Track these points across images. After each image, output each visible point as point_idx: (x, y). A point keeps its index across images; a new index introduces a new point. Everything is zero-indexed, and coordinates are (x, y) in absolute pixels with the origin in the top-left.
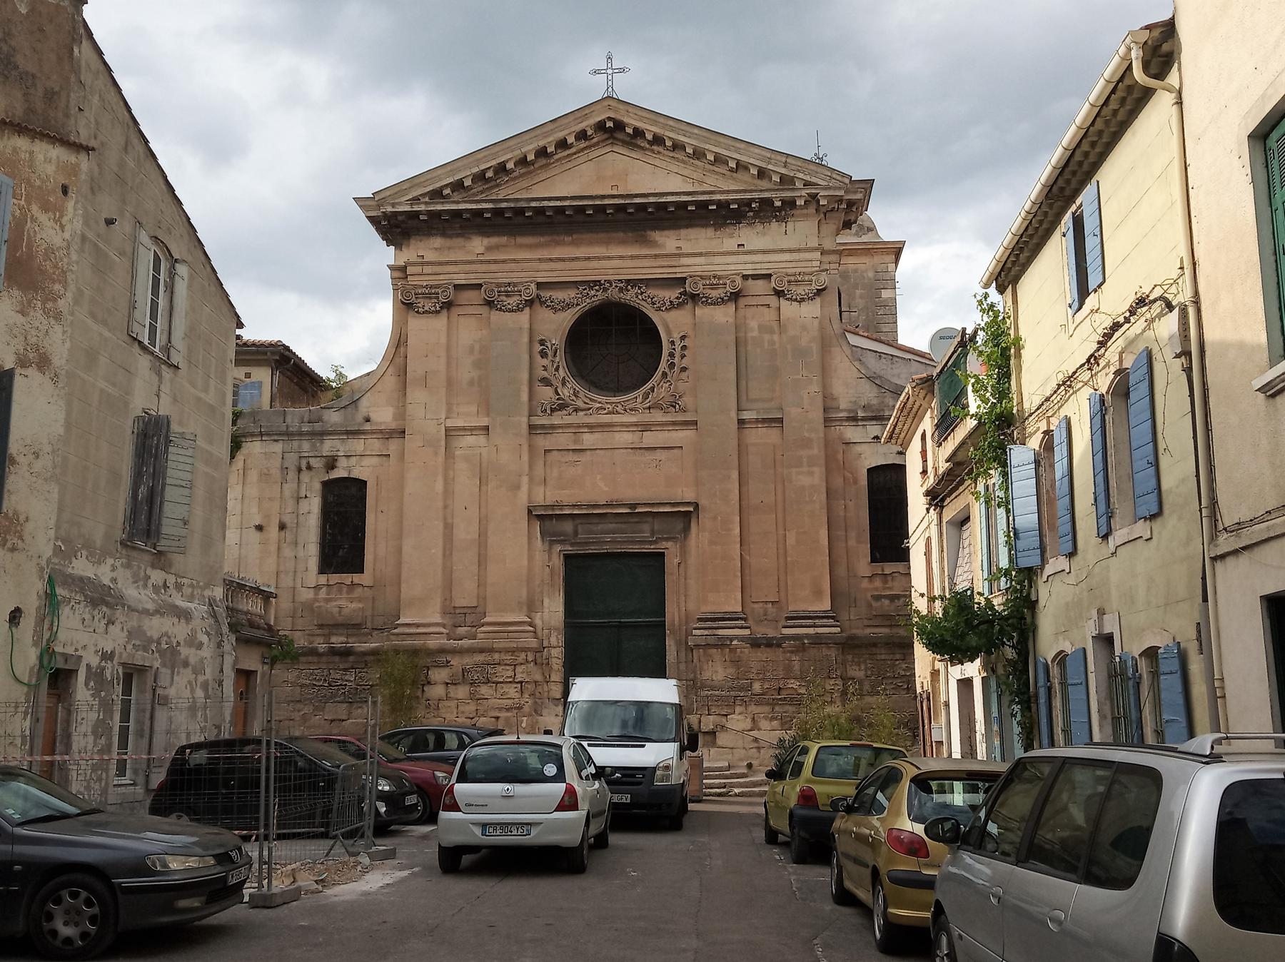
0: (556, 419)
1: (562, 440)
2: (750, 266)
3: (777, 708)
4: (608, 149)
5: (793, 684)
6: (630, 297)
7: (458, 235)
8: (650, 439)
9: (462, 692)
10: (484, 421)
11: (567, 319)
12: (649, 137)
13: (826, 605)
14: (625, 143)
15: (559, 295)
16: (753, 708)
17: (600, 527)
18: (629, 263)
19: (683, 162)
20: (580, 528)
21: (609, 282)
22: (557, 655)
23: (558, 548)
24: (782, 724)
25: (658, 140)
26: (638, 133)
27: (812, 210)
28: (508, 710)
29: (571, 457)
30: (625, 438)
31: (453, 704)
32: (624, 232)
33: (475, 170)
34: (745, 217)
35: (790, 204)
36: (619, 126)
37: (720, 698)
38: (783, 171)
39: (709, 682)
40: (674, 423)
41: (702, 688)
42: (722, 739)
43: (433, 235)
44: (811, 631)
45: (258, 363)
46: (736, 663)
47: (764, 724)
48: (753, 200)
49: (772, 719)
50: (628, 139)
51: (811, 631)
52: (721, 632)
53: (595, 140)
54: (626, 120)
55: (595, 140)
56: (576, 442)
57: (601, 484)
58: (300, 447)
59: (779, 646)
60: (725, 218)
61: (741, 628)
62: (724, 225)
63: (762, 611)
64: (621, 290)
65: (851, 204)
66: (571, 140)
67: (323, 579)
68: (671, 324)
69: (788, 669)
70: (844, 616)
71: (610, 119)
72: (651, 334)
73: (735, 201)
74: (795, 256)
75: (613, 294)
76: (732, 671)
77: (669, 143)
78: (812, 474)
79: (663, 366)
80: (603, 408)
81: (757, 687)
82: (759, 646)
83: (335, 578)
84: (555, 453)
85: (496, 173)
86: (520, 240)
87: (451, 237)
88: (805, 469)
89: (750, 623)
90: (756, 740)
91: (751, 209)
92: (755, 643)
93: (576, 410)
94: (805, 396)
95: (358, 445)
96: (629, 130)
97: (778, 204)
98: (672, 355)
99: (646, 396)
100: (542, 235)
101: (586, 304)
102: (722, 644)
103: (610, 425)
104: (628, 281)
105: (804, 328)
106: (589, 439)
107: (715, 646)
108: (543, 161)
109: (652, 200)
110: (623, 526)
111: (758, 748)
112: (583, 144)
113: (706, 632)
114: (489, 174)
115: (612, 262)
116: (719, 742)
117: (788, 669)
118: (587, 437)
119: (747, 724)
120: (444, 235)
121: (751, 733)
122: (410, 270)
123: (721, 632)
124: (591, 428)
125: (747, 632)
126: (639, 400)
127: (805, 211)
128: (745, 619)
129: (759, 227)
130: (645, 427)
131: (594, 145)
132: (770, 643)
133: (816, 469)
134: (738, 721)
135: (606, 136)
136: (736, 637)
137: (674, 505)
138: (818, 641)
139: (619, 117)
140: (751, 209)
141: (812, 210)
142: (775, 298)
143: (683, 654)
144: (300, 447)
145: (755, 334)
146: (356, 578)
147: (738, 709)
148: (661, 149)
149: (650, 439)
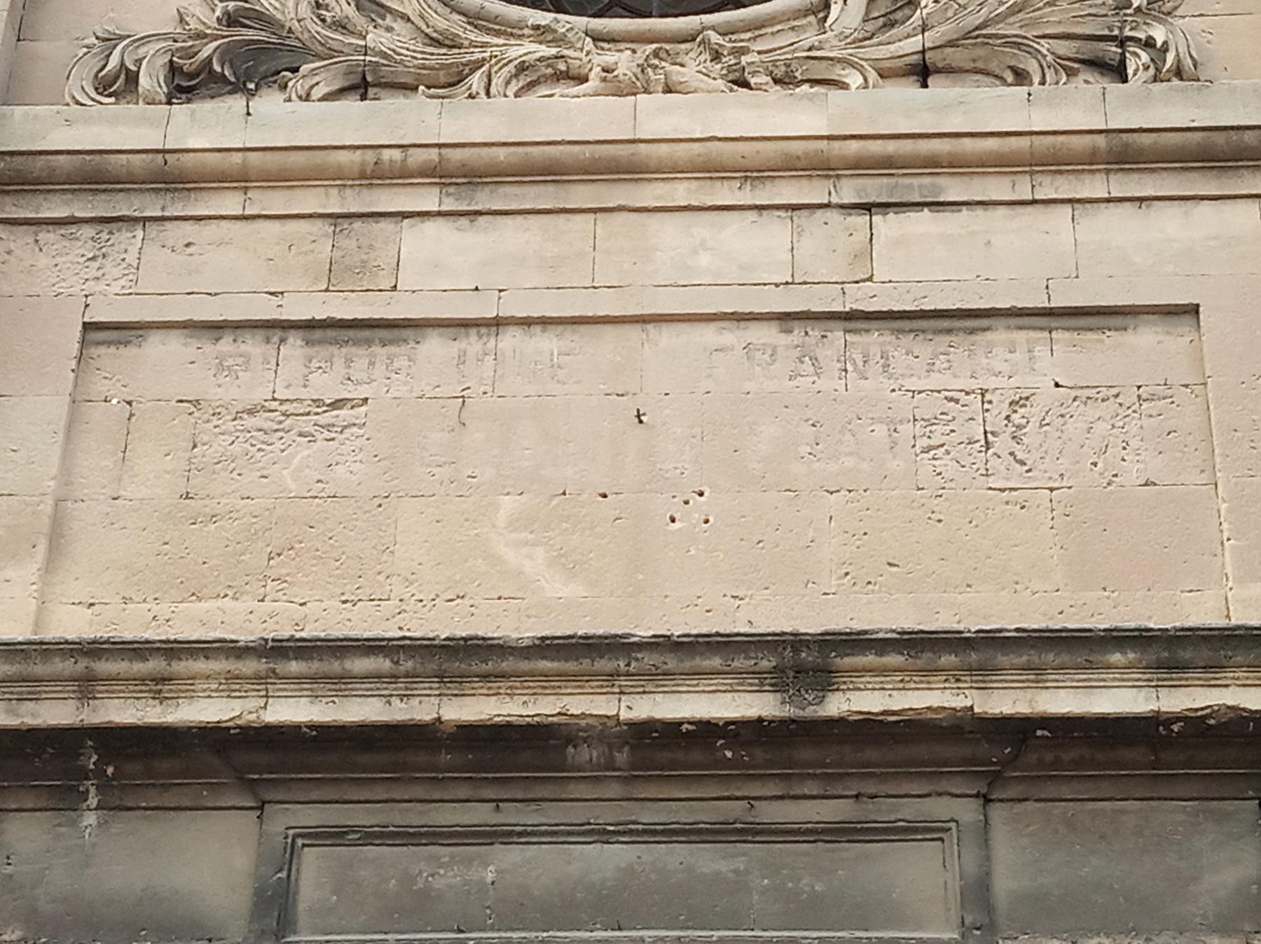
0: (207, 127)
1: (235, 261)
8: (921, 256)
17: (499, 865)
20: (315, 872)
29: (295, 371)
30: (749, 252)
40: (1124, 153)
57: (535, 563)
84: (158, 347)
93: (361, 85)
103: (619, 166)
106: (437, 261)
110: (709, 860)
118: (419, 243)
124: (468, 180)
130: (892, 177)
137: (1170, 651)
149: (921, 256)
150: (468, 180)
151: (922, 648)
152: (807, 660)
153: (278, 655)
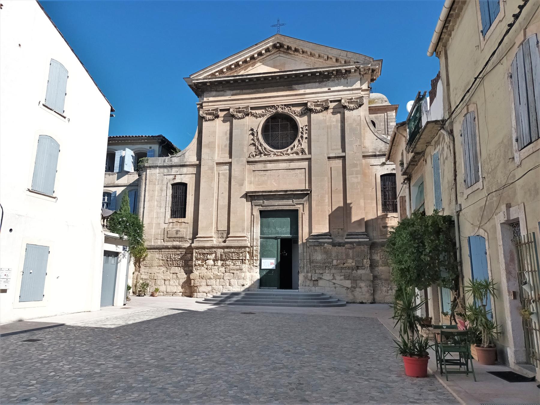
2: (333, 97)
3: (343, 271)
4: (278, 55)
5: (350, 261)
6: (286, 110)
7: (222, 91)
9: (220, 263)
10: (230, 160)
11: (263, 120)
12: (293, 49)
13: (363, 230)
14: (284, 52)
15: (259, 112)
16: (333, 271)
18: (285, 98)
19: (307, 58)
21: (278, 106)
22: (257, 249)
23: (258, 207)
24: (345, 278)
25: (296, 50)
26: (289, 48)
27: (357, 74)
28: (237, 270)
29: (262, 173)
31: (216, 267)
32: (284, 86)
33: (227, 65)
34: (331, 78)
35: (348, 71)
36: (282, 46)
37: (320, 267)
38: (346, 58)
39: (315, 260)
41: (313, 262)
42: (321, 283)
43: (211, 91)
44: (357, 240)
45: (154, 143)
46: (326, 252)
47: (338, 277)
48: (333, 70)
49: (341, 276)
50: (285, 51)
51: (357, 240)
52: (320, 240)
53: (273, 52)
54: (284, 43)
55: (273, 52)
56: (264, 167)
58: (164, 171)
59: (344, 246)
60: (323, 78)
61: (329, 239)
62: (323, 81)
63: (337, 233)
64: (282, 109)
65: (373, 71)
66: (263, 52)
67: (171, 220)
68: (302, 122)
69: (347, 255)
70: (371, 234)
71: (278, 43)
72: (294, 126)
73: (326, 71)
74: (351, 92)
75: (280, 110)
76: (324, 256)
77: (301, 51)
78: (357, 177)
79: (299, 137)
80: (274, 154)
81: (335, 262)
82: (335, 246)
83: (175, 220)
85: (235, 66)
86: (244, 91)
87: (219, 91)
88: (354, 176)
89: (333, 237)
90: (334, 284)
91: (333, 75)
92: (334, 245)
94: (355, 147)
95: (185, 170)
96: (286, 47)
97: (344, 71)
98: (302, 133)
99: (292, 149)
100: (253, 89)
101: (268, 115)
102: (321, 244)
104: (285, 105)
105: (354, 120)
106: (269, 166)
107: (318, 246)
108: (253, 61)
109: (294, 72)
111: (335, 287)
112: (268, 54)
113: (314, 240)
114: (233, 67)
115: (279, 99)
116: (319, 284)
117: (347, 255)
119: (331, 277)
120: (216, 91)
121: (333, 281)
122: (204, 104)
123: (320, 240)
124: (271, 161)
125: (331, 240)
126: (289, 150)
127: (355, 74)
128: (330, 236)
129: (337, 82)
131: (272, 54)
132: (340, 245)
133: (358, 176)
134: (327, 276)
135: (277, 50)
136: (326, 242)
138: (359, 244)
139: (281, 42)
140: (333, 75)
141: (357, 74)
142: (343, 109)
143: (305, 249)
144: (164, 171)
145: (335, 123)
146: (183, 220)
147: (327, 271)
148: (298, 53)
149: (293, 165)
150: (271, 161)
151: (291, 191)
152: (286, 191)
153: (263, 192)
